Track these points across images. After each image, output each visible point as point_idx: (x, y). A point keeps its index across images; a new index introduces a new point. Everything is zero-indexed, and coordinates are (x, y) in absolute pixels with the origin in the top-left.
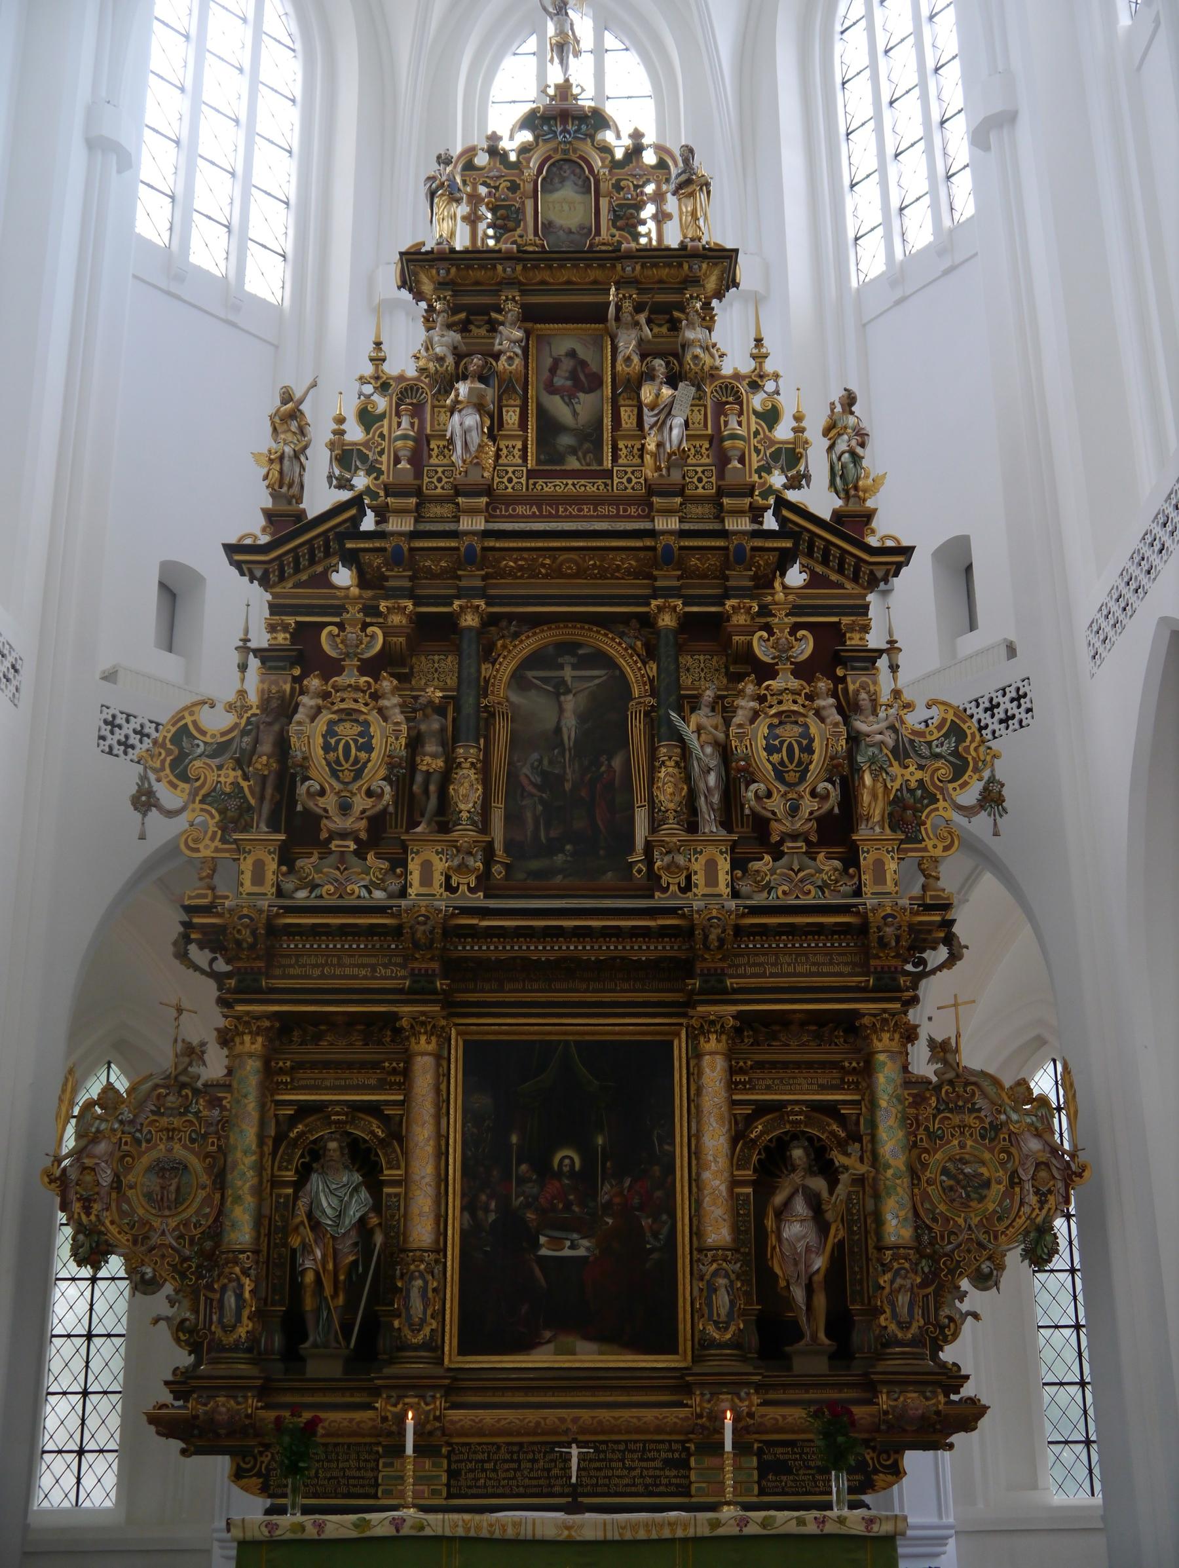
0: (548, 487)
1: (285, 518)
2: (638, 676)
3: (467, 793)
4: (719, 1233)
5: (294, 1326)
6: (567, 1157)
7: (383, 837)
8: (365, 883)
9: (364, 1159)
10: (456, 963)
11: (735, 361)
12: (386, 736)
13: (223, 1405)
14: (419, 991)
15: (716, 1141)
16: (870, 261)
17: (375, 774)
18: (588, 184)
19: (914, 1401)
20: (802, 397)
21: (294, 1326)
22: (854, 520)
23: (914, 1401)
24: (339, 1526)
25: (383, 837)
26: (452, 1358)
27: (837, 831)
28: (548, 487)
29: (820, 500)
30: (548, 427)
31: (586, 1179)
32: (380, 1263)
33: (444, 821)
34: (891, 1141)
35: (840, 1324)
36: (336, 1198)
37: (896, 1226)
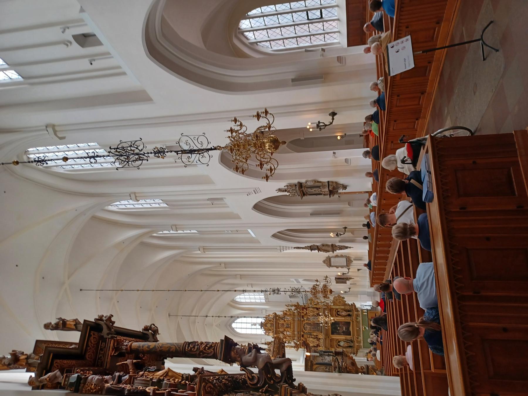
0: (292, 327)
1: (294, 347)
2: (306, 322)
3: (315, 334)
4: (343, 318)
5: (350, 347)
6: (339, 328)
7: (318, 339)
8: (322, 341)
9: (339, 342)
10: (327, 335)
11: (282, 313)
12: (311, 339)
13: (355, 350)
14: (329, 337)
15: (338, 318)
16: (264, 301)
17: (313, 340)
18: (267, 323)
19: (353, 307)
20: (285, 309)
21: (350, 347)
22: (295, 306)
23: (353, 307)
24: (362, 342)
25: (318, 339)
26: (352, 336)
27: (317, 309)
28: (292, 327)
29: (293, 308)
30: (287, 327)
31: (340, 327)
32: (346, 341)
33: (317, 336)
34: (337, 307)
35: (349, 311)
36: (342, 344)
37: (343, 307)
